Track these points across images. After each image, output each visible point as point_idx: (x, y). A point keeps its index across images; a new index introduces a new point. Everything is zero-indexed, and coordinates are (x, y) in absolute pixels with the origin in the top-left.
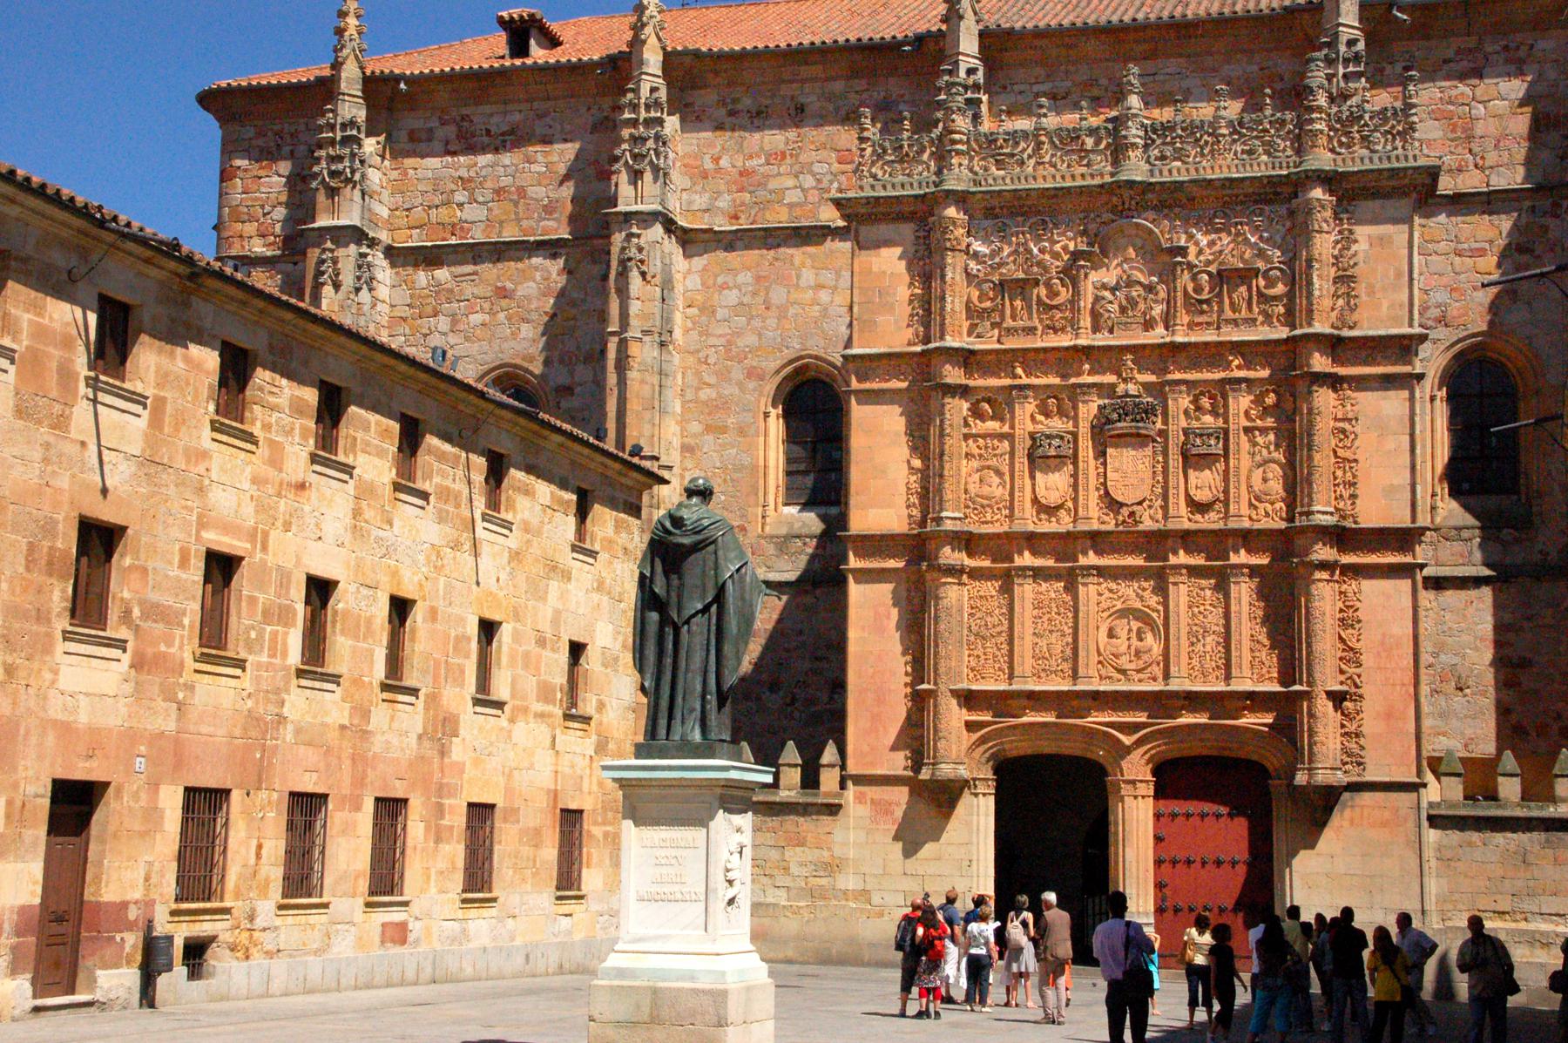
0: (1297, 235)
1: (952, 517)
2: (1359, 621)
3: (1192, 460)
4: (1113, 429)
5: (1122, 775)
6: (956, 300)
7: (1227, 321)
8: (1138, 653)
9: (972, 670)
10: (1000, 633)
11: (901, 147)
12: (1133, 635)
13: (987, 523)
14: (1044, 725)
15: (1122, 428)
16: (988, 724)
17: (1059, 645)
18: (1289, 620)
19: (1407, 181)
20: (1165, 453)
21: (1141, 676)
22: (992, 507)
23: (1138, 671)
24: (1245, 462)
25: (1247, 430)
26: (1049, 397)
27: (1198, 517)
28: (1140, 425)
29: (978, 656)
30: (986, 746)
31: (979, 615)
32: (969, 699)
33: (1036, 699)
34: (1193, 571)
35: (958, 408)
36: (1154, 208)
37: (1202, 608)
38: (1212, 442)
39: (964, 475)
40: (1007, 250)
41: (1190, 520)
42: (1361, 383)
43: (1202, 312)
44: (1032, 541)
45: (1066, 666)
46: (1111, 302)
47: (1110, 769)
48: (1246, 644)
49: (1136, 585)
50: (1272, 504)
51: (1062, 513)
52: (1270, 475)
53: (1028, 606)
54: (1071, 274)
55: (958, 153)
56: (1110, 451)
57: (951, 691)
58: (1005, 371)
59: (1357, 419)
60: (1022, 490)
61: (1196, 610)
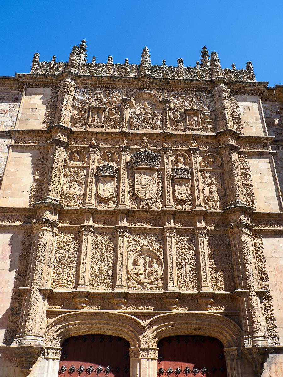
0: (216, 98)
1: (53, 196)
2: (264, 258)
3: (175, 181)
4: (139, 165)
5: (140, 345)
6: (67, 111)
7: (189, 129)
8: (150, 274)
9: (55, 281)
10: (72, 262)
11: (50, 65)
12: (147, 264)
13: (71, 206)
14: (95, 313)
15: (142, 165)
16: (60, 313)
17: (105, 268)
18: (230, 256)
19: (256, 88)
20: (163, 178)
21: (151, 286)
22: (75, 199)
23: (150, 283)
24: (201, 185)
25: (202, 171)
26: (107, 152)
27: (180, 207)
28: (151, 164)
29: (59, 274)
30: (58, 327)
31: (62, 251)
32: (50, 296)
33: (90, 298)
34: (178, 232)
35: (61, 154)
36: (157, 90)
37: (183, 251)
38: (186, 173)
39: (62, 184)
40: (91, 99)
41: (175, 208)
42: (250, 155)
43: (178, 125)
44: (94, 213)
45: (109, 280)
46: (137, 119)
47: (131, 342)
48: (208, 269)
49: (149, 238)
50: (215, 202)
51: (111, 203)
52: (213, 190)
53: (90, 247)
54: (120, 108)
55: (74, 67)
56: (136, 175)
57: (40, 290)
58: (87, 142)
59: (249, 169)
60: (91, 190)
61: (181, 251)
